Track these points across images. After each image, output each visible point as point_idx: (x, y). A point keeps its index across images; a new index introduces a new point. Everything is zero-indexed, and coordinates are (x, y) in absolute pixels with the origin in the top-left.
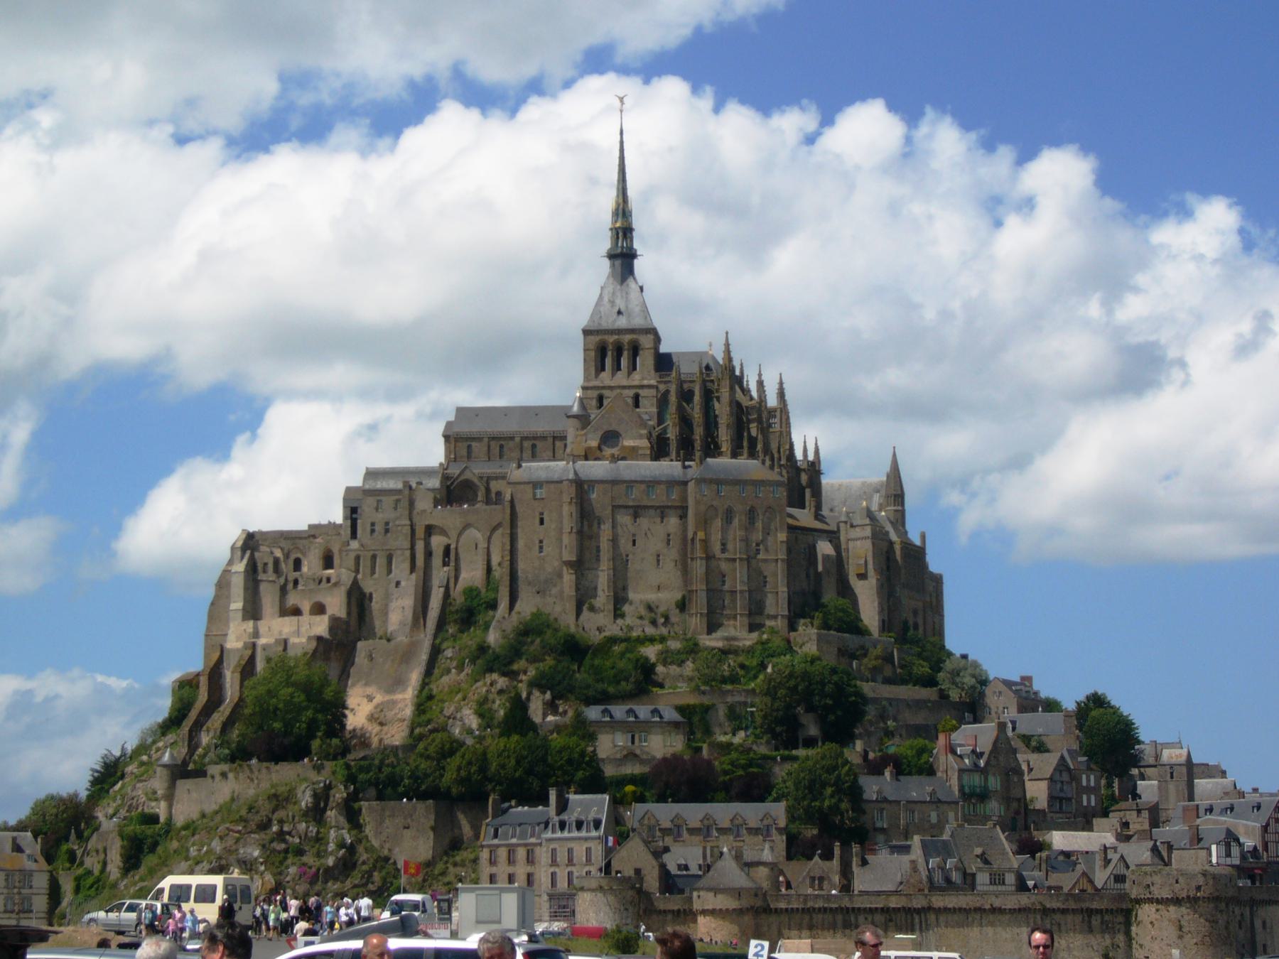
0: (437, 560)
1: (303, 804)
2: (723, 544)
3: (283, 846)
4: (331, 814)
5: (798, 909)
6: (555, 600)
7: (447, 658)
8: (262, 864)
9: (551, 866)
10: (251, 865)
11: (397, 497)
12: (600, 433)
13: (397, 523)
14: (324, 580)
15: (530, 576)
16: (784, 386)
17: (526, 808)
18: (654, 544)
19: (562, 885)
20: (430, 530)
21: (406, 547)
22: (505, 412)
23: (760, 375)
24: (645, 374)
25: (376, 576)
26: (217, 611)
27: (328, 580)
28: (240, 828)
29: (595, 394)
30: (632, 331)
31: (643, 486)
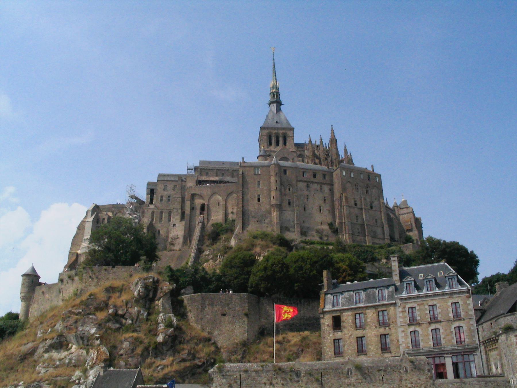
1: (136, 293)
2: (355, 201)
3: (117, 326)
4: (159, 303)
6: (267, 225)
7: (206, 255)
8: (97, 339)
9: (410, 325)
10: (88, 341)
11: (175, 184)
13: (175, 196)
15: (253, 213)
16: (352, 157)
17: (356, 282)
20: (193, 196)
21: (179, 208)
22: (223, 163)
23: (345, 147)
25: (163, 222)
26: (76, 241)
28: (81, 311)
30: (284, 129)
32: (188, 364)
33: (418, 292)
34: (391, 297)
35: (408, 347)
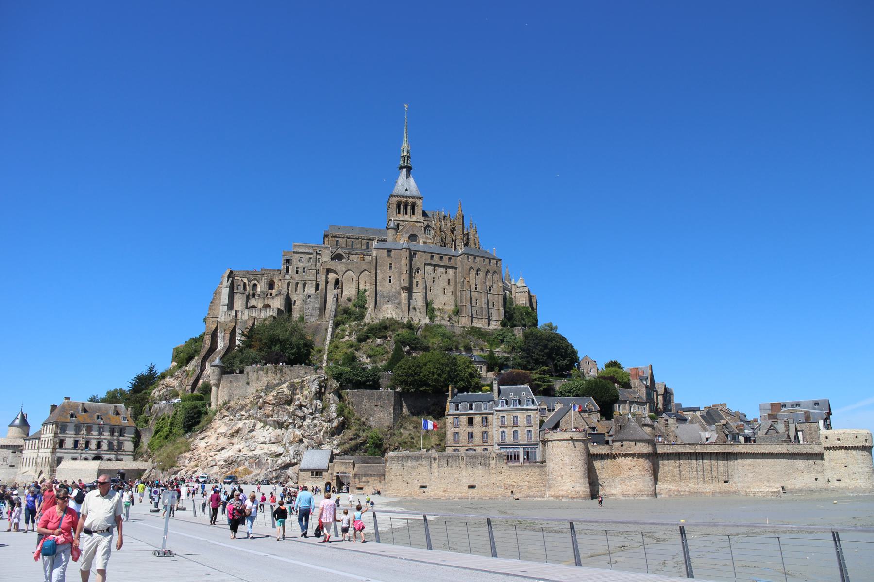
0: (331, 286)
1: (313, 390)
2: (476, 285)
5: (673, 453)
9: (500, 427)
11: (311, 256)
12: (408, 235)
14: (269, 294)
18: (442, 283)
19: (509, 439)
24: (418, 216)
25: (297, 293)
27: (271, 294)
29: (396, 223)
30: (413, 198)
31: (438, 256)
32: (353, 443)
33: (508, 407)
34: (491, 408)
35: (499, 440)
